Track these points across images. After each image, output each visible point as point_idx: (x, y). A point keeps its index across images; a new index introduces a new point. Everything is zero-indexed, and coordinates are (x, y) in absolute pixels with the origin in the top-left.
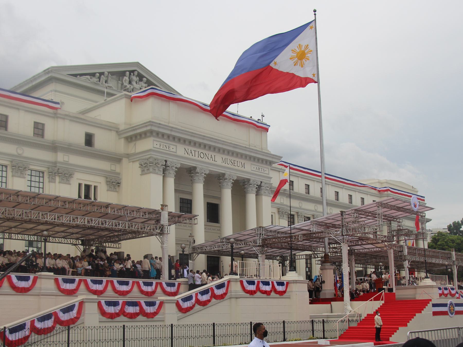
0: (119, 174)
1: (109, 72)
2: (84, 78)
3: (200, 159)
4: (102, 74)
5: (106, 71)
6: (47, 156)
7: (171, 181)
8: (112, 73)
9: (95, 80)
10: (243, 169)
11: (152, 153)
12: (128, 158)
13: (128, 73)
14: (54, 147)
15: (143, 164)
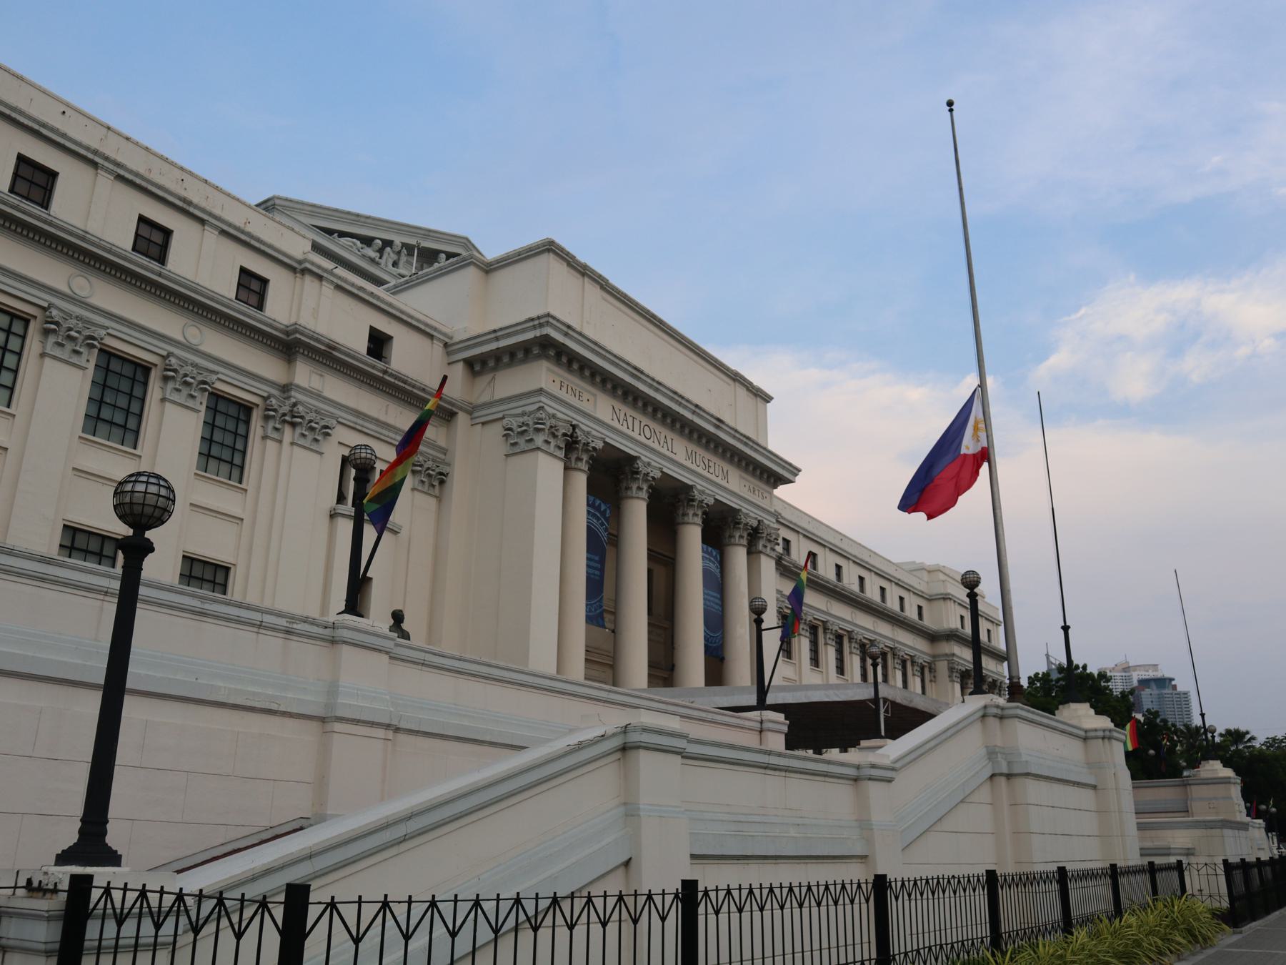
0: (444, 451)
1: (404, 245)
2: (344, 241)
3: (642, 439)
4: (388, 243)
5: (398, 240)
6: (266, 365)
7: (580, 481)
8: (409, 248)
9: (370, 252)
10: (723, 483)
11: (543, 399)
12: (470, 413)
13: (443, 256)
14: (289, 345)
15: (514, 426)
